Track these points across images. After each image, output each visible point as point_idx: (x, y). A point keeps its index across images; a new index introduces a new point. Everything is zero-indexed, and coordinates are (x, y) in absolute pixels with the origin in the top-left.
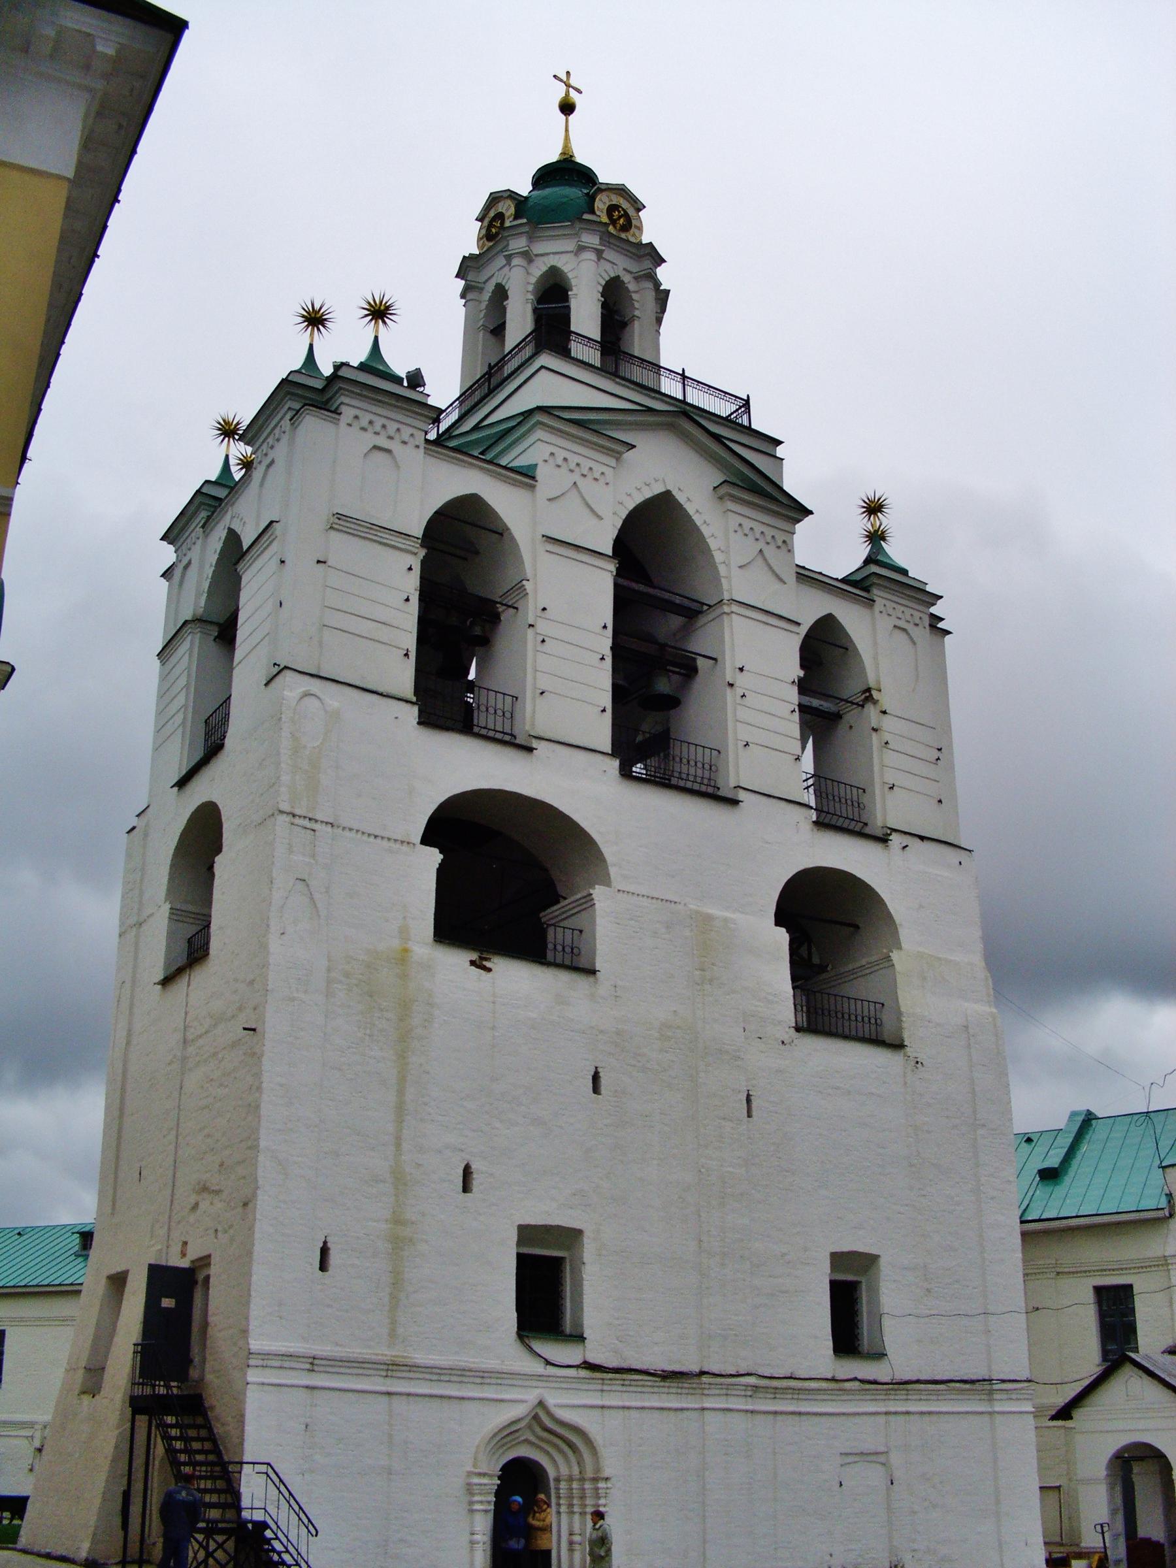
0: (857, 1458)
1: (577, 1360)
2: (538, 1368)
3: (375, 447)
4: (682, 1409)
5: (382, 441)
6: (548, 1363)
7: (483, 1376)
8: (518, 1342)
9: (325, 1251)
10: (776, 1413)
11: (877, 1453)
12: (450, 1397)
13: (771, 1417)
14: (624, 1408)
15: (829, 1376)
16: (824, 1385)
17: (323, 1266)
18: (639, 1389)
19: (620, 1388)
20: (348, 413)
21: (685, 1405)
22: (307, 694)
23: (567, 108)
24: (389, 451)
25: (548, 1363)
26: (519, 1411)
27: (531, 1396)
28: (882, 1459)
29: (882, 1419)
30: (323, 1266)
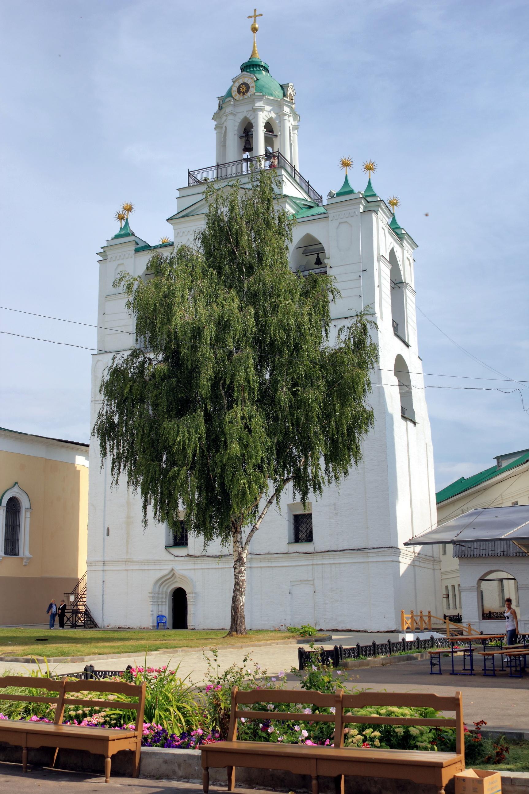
0: (299, 583)
1: (185, 554)
2: (172, 558)
3: (119, 265)
4: (223, 568)
5: (120, 262)
6: (175, 556)
7: (155, 562)
8: (166, 551)
9: (108, 530)
10: (261, 567)
11: (308, 581)
12: (145, 570)
13: (260, 569)
14: (202, 569)
15: (286, 552)
16: (281, 555)
17: (108, 535)
18: (208, 562)
19: (200, 562)
20: (109, 257)
21: (224, 566)
22: (98, 361)
23: (254, 30)
24: (123, 264)
25: (175, 556)
26: (166, 572)
27: (169, 567)
28: (312, 583)
29: (310, 567)
30: (108, 535)
